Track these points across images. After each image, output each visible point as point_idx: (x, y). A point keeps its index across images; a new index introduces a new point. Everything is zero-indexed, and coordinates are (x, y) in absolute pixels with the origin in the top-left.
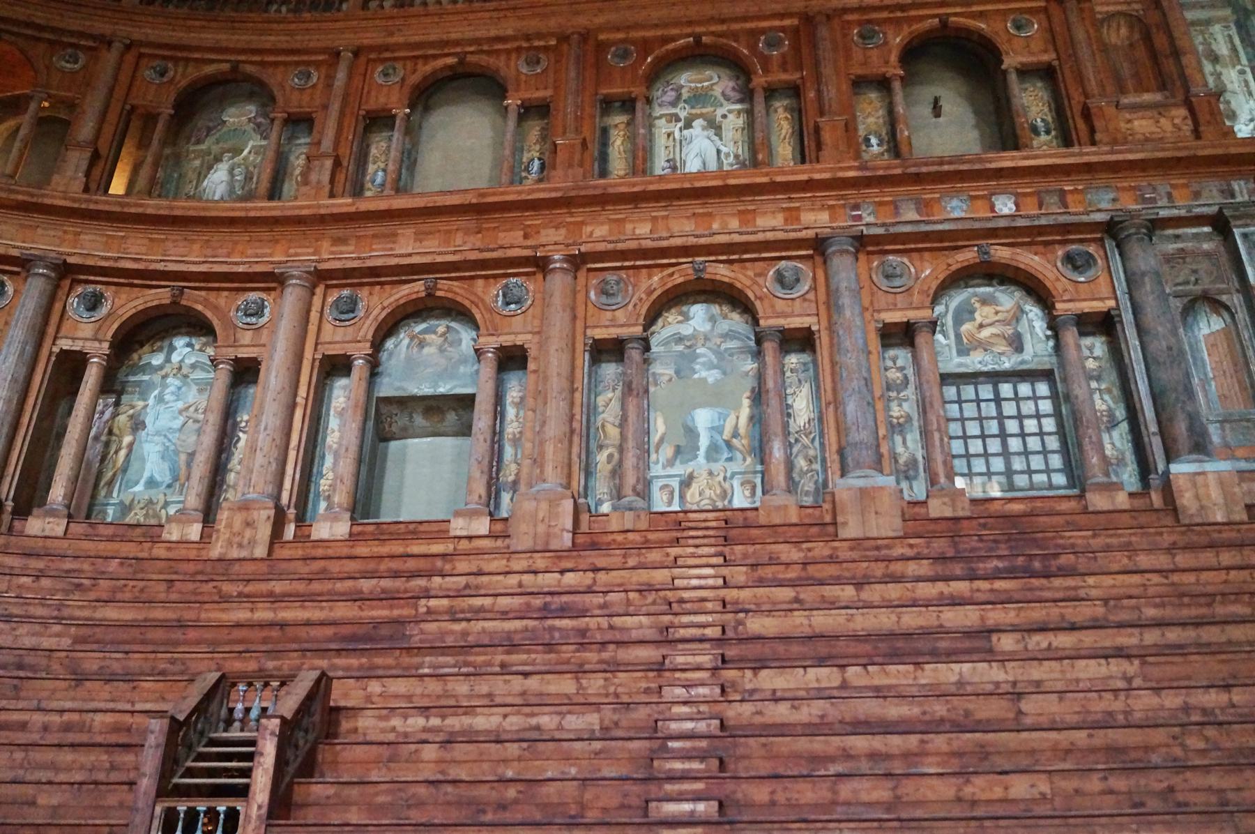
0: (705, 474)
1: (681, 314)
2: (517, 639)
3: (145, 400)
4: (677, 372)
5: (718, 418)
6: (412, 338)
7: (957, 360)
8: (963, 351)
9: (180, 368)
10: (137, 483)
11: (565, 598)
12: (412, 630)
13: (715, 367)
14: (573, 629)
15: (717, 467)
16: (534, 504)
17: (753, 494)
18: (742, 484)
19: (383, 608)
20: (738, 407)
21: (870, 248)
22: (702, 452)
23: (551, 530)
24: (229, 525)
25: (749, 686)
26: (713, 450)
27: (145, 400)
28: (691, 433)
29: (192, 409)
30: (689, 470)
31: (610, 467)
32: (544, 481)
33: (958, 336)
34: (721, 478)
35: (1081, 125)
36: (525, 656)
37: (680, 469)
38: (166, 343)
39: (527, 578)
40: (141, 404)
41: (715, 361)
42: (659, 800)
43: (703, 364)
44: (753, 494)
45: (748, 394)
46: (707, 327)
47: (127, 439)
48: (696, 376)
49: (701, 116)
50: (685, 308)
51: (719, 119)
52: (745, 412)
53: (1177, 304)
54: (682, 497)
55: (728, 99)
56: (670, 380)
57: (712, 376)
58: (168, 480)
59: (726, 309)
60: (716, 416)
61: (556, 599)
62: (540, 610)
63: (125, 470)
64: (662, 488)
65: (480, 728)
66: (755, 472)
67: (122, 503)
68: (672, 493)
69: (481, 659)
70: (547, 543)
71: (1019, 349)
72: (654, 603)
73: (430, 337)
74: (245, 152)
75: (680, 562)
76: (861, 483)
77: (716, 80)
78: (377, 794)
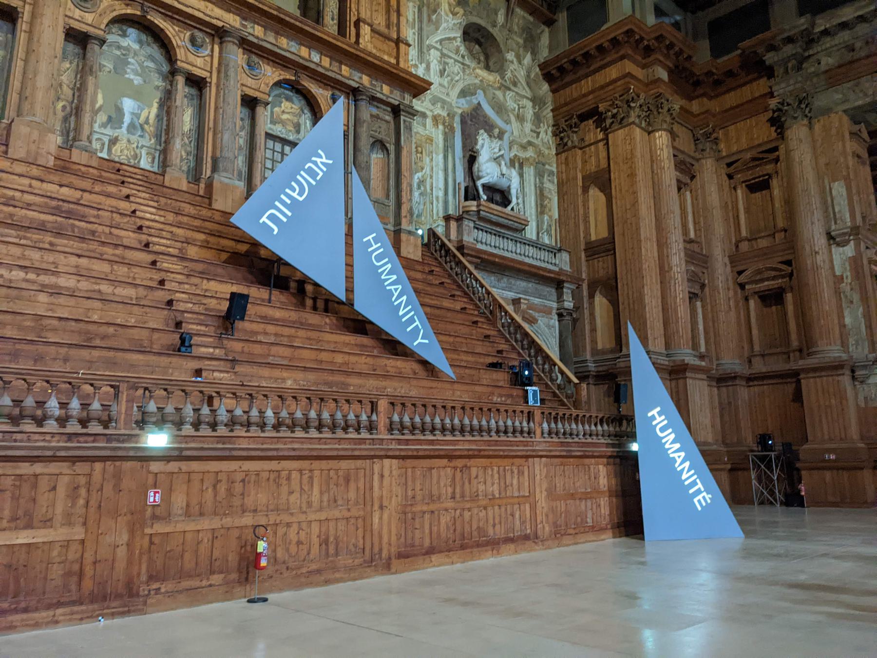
0: (125, 141)
1: (121, 30)
2: (49, 225)
5: (138, 108)
7: (269, 126)
8: (273, 122)
11: (72, 206)
14: (86, 229)
16: (28, 129)
17: (153, 162)
18: (147, 154)
21: (246, 47)
22: (125, 125)
23: (40, 151)
25: (204, 287)
26: (132, 127)
28: (120, 111)
30: (116, 134)
31: (63, 114)
33: (272, 112)
34: (135, 146)
35: (353, 28)
36: (66, 242)
37: (108, 131)
39: (35, 183)
41: (140, 71)
42: (198, 345)
43: (133, 70)
44: (153, 162)
45: (157, 100)
48: (127, 76)
50: (124, 28)
52: (154, 110)
53: (372, 140)
54: (110, 150)
56: (110, 72)
57: (137, 80)
59: (150, 39)
60: (136, 106)
61: (65, 204)
62: (54, 208)
64: (97, 139)
65: (62, 285)
66: (156, 149)
68: (103, 145)
69: (35, 237)
70: (36, 159)
71: (298, 132)
72: (128, 222)
75: (132, 199)
76: (227, 181)
78: (25, 320)
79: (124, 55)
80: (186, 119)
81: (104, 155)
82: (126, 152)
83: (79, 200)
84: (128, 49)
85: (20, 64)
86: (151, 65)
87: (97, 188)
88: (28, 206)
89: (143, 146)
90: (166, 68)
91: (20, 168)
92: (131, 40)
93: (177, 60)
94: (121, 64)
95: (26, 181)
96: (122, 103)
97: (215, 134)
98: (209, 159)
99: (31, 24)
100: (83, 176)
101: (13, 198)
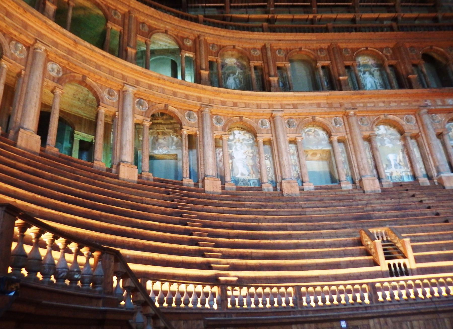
4: (381, 144)
6: (305, 133)
9: (239, 140)
13: (390, 143)
20: (399, 154)
22: (393, 166)
26: (396, 166)
28: (389, 161)
29: (247, 152)
45: (400, 150)
46: (385, 132)
49: (367, 71)
50: (378, 126)
51: (372, 72)
55: (374, 66)
57: (390, 146)
66: (408, 171)
73: (310, 133)
74: (237, 74)
77: (368, 60)
80: (416, 154)
84: (382, 134)
85: (354, 156)
89: (403, 172)
92: (382, 130)
94: (382, 141)
97: (432, 156)
98: (434, 168)
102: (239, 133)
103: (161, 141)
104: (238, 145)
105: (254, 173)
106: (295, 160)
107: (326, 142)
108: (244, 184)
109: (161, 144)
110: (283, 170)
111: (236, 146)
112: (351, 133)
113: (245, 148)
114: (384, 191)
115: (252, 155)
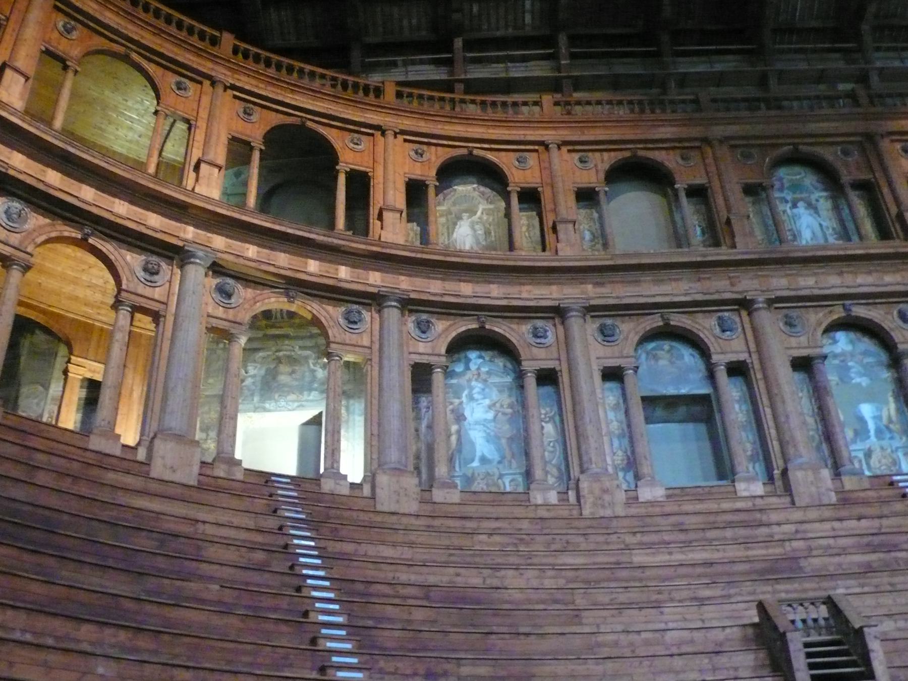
0: (878, 450)
1: (830, 338)
2: (875, 565)
3: (459, 398)
4: (841, 379)
6: (648, 353)
9: (479, 374)
10: (473, 460)
12: (803, 563)
13: (864, 375)
15: (885, 443)
19: (762, 548)
20: (887, 403)
22: (872, 433)
24: (591, 492)
26: (879, 433)
27: (459, 398)
28: (861, 420)
29: (498, 405)
30: (867, 446)
32: (801, 457)
34: (889, 450)
38: (462, 355)
39: (837, 525)
40: (457, 401)
41: (863, 371)
45: (890, 393)
46: (849, 348)
47: (454, 428)
48: (854, 381)
50: (832, 334)
52: (892, 406)
56: (837, 384)
57: (864, 381)
58: (497, 457)
59: (859, 335)
63: (459, 450)
67: (465, 475)
70: (820, 500)
73: (660, 353)
79: (843, 361)
81: (867, 473)
82: (884, 461)
83: (880, 529)
84: (843, 354)
85: (768, 411)
86: (870, 360)
87: (886, 510)
88: (843, 552)
89: (897, 448)
90: (884, 357)
91: (813, 514)
92: (843, 342)
93: (896, 344)
94: (844, 370)
95: (827, 526)
96: (860, 411)
99: (764, 369)
100: (866, 503)
101: (829, 547)
102: (480, 357)
103: (283, 378)
104: (477, 386)
105: (513, 456)
106: (621, 422)
107: (701, 375)
108: (487, 485)
109: (284, 385)
110: (583, 447)
111: (471, 388)
112: (759, 351)
113: (495, 395)
114: (845, 500)
115: (510, 411)
